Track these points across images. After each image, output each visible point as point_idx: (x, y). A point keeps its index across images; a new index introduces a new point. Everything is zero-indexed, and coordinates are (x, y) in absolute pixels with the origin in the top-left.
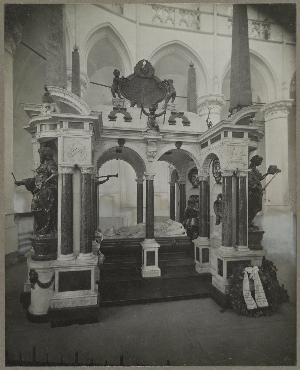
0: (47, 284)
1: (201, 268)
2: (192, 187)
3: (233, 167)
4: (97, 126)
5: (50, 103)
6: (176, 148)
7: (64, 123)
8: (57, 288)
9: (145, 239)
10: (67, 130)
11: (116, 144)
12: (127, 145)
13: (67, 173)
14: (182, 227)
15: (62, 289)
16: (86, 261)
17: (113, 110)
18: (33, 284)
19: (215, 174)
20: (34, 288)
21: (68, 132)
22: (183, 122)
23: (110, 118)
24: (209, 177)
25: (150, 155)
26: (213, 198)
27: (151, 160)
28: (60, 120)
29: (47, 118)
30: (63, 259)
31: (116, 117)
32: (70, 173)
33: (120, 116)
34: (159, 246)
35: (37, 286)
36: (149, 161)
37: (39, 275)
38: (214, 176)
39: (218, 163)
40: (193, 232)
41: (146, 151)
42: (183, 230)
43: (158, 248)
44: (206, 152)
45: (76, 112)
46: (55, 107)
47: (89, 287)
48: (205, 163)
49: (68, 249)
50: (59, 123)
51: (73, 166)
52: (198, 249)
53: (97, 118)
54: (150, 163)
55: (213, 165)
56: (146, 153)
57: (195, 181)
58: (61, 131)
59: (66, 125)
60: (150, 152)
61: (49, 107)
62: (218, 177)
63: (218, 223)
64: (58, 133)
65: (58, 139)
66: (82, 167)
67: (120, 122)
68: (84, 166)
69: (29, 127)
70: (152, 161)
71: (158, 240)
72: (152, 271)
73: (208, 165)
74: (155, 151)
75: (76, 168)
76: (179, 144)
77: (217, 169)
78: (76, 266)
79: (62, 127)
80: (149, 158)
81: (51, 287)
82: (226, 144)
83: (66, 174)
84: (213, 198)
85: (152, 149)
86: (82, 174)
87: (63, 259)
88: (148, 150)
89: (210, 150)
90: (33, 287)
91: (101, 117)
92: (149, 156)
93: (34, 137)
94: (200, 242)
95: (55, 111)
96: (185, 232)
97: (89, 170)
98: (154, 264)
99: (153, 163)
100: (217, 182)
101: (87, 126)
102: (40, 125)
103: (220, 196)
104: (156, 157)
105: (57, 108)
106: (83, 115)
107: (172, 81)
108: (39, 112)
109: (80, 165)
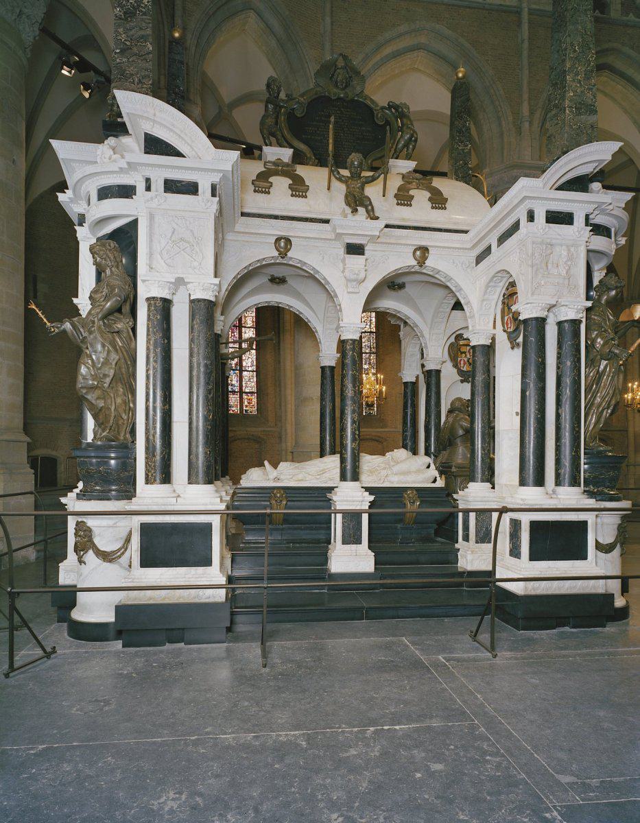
0: (113, 552)
1: (472, 557)
15: (147, 562)
24: (493, 339)
30: (149, 495)
35: (90, 556)
36: (349, 293)
37: (96, 531)
38: (505, 331)
40: (456, 475)
48: (483, 300)
72: (351, 559)
80: (349, 284)
81: (124, 560)
87: (149, 495)
94: (474, 495)
96: (438, 476)
98: (359, 541)
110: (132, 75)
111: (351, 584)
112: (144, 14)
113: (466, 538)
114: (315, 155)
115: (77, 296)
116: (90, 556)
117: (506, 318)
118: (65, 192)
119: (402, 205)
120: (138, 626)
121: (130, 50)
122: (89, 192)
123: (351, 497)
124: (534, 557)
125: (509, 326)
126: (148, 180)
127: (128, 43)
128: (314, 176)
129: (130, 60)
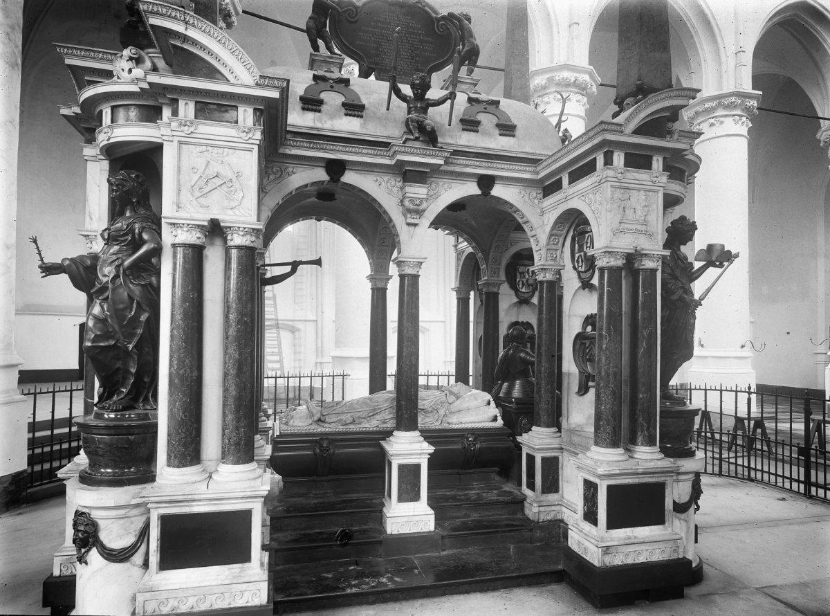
1: (536, 507)
2: (515, 300)
4: (271, 116)
5: (142, 49)
6: (479, 192)
7: (181, 103)
8: (154, 559)
9: (395, 433)
10: (192, 122)
11: (321, 175)
12: (349, 177)
13: (187, 242)
14: (489, 403)
16: (237, 486)
17: (313, 83)
18: (83, 550)
19: (578, 262)
20: (86, 563)
21: (192, 129)
24: (558, 272)
25: (412, 207)
26: (572, 327)
27: (410, 221)
28: (172, 95)
29: (135, 89)
31: (321, 102)
32: (198, 242)
33: (333, 99)
34: (431, 449)
35: (94, 555)
36: (409, 224)
37: (102, 523)
38: (574, 268)
39: (587, 235)
40: (519, 416)
41: (400, 197)
42: (493, 410)
43: (429, 454)
44: (555, 206)
45: (212, 72)
46: (156, 60)
49: (188, 450)
50: (167, 104)
51: (206, 224)
52: (531, 459)
53: (275, 94)
54: (412, 228)
56: (402, 201)
57: (523, 285)
58: (174, 124)
59: (187, 109)
60: (412, 200)
61: (138, 61)
62: (585, 272)
63: (583, 390)
64: (164, 131)
65: (164, 146)
66: (230, 227)
68: (238, 225)
69: (78, 110)
70: (415, 225)
71: (429, 436)
72: (409, 517)
73: (561, 239)
74: (425, 196)
75: (215, 230)
76: (486, 182)
77: (585, 250)
78: (211, 500)
79: (175, 113)
80: (409, 216)
81: (138, 558)
83: (184, 245)
84: (572, 327)
85: (417, 191)
86: (231, 247)
88: (407, 195)
89: (566, 199)
90: (82, 559)
91: (285, 92)
92: (409, 211)
93: (91, 140)
94: (536, 440)
95: (155, 69)
96: (498, 415)
97: (249, 237)
98: (416, 498)
99: (418, 229)
100: (582, 282)
101: (246, 115)
102: (113, 108)
103: (589, 320)
104: (426, 214)
105: (161, 64)
106: (234, 85)
107: (469, 20)
108: (109, 74)
109: (224, 221)
113: (531, 486)
116: (94, 555)
117: (577, 255)
124: (611, 525)
125: (580, 264)
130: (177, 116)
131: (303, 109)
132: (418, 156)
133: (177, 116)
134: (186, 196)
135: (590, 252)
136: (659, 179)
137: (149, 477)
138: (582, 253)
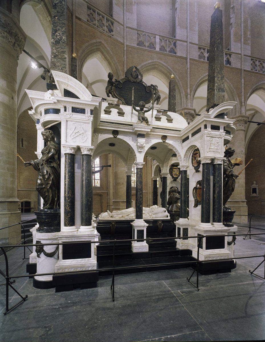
1: (181, 244)
3: (212, 155)
6: (162, 141)
8: (61, 256)
14: (165, 212)
15: (66, 257)
16: (88, 232)
18: (39, 253)
19: (194, 164)
20: (40, 257)
22: (167, 119)
23: (105, 112)
26: (192, 185)
27: (140, 150)
30: (66, 230)
34: (147, 225)
38: (193, 166)
40: (175, 216)
42: (167, 213)
47: (90, 256)
49: (71, 222)
51: (76, 147)
52: (179, 229)
55: (193, 156)
63: (196, 206)
67: (114, 116)
72: (140, 247)
73: (189, 156)
76: (164, 137)
77: (197, 159)
78: (78, 237)
81: (56, 256)
82: (206, 135)
83: (68, 154)
84: (192, 185)
85: (141, 141)
87: (66, 230)
90: (38, 256)
94: (181, 222)
103: (199, 183)
107: (157, 87)
109: (81, 146)
110: (59, 66)
111: (141, 255)
112: (63, 43)
114: (125, 101)
115: (36, 151)
117: (194, 162)
118: (31, 110)
119: (157, 120)
120: (62, 282)
121: (57, 57)
122: (41, 111)
123: (140, 224)
125: (195, 164)
126: (65, 107)
127: (57, 54)
128: (127, 109)
129: (58, 60)
130: (66, 111)
131: (105, 113)
132: (143, 128)
133: (66, 111)
134: (69, 139)
135: (199, 159)
136: (222, 134)
137: (59, 230)
138: (196, 161)
